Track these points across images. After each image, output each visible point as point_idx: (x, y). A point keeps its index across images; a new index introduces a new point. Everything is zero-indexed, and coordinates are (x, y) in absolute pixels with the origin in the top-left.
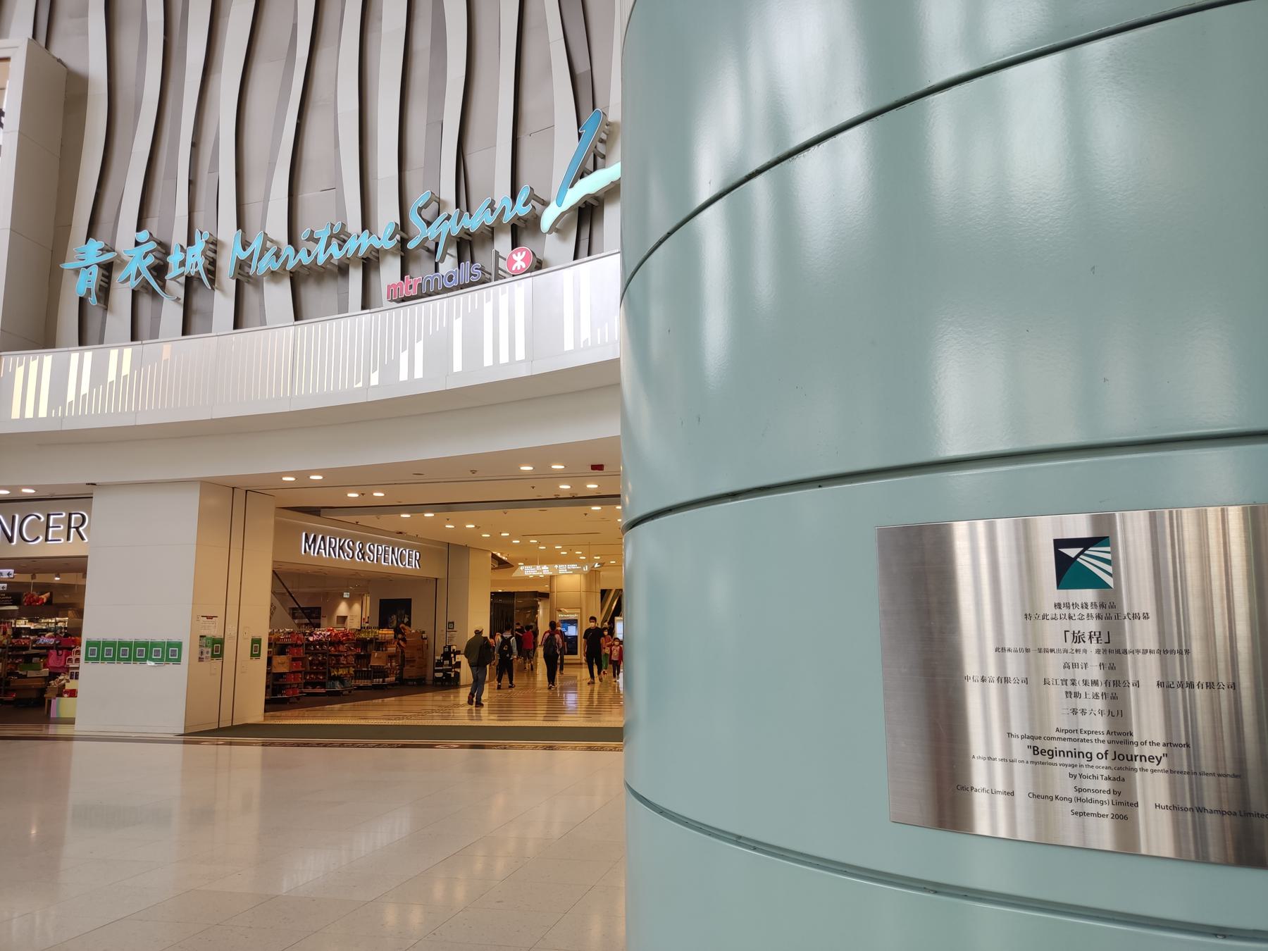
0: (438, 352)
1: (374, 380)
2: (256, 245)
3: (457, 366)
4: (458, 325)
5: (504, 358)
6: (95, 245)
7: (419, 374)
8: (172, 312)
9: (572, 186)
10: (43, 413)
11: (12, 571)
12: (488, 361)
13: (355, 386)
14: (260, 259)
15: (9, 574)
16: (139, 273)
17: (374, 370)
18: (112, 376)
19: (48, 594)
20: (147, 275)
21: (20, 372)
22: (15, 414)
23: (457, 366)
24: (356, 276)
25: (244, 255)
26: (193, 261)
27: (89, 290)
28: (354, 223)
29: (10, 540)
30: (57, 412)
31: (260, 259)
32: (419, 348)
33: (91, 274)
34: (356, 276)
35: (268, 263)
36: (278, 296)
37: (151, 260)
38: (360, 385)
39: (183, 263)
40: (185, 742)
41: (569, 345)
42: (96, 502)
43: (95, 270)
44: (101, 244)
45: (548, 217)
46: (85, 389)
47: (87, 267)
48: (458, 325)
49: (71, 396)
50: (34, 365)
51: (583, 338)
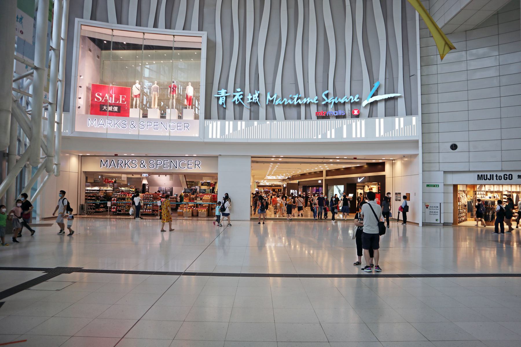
0: (339, 131)
1: (320, 137)
2: (275, 96)
3: (345, 136)
4: (345, 127)
5: (359, 136)
6: (223, 92)
7: (333, 136)
8: (246, 113)
9: (371, 97)
10: (218, 137)
11: (147, 174)
12: (354, 136)
13: (314, 138)
14: (276, 101)
15: (146, 175)
16: (238, 100)
17: (320, 134)
18: (239, 128)
19: (114, 180)
20: (240, 100)
21: (211, 125)
22: (210, 136)
23: (345, 136)
24: (303, 108)
25: (271, 99)
26: (255, 98)
27: (223, 103)
28: (302, 94)
29: (176, 168)
30: (223, 137)
31: (276, 101)
32: (333, 131)
33: (223, 99)
34: (303, 108)
35: (277, 103)
36: (279, 111)
37: (241, 97)
38: (315, 137)
39: (252, 99)
40: (250, 221)
41: (377, 135)
42: (220, 159)
43: (224, 98)
44: (226, 91)
45: (364, 103)
46: (231, 131)
47: (222, 97)
48: (345, 127)
49: (227, 133)
50: (215, 124)
51: (381, 135)
